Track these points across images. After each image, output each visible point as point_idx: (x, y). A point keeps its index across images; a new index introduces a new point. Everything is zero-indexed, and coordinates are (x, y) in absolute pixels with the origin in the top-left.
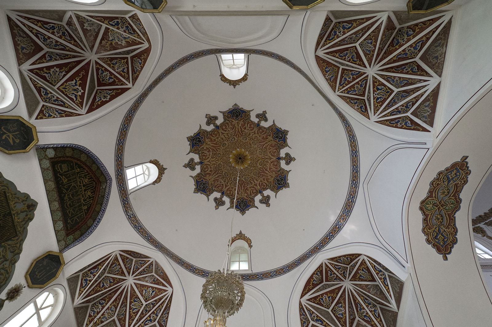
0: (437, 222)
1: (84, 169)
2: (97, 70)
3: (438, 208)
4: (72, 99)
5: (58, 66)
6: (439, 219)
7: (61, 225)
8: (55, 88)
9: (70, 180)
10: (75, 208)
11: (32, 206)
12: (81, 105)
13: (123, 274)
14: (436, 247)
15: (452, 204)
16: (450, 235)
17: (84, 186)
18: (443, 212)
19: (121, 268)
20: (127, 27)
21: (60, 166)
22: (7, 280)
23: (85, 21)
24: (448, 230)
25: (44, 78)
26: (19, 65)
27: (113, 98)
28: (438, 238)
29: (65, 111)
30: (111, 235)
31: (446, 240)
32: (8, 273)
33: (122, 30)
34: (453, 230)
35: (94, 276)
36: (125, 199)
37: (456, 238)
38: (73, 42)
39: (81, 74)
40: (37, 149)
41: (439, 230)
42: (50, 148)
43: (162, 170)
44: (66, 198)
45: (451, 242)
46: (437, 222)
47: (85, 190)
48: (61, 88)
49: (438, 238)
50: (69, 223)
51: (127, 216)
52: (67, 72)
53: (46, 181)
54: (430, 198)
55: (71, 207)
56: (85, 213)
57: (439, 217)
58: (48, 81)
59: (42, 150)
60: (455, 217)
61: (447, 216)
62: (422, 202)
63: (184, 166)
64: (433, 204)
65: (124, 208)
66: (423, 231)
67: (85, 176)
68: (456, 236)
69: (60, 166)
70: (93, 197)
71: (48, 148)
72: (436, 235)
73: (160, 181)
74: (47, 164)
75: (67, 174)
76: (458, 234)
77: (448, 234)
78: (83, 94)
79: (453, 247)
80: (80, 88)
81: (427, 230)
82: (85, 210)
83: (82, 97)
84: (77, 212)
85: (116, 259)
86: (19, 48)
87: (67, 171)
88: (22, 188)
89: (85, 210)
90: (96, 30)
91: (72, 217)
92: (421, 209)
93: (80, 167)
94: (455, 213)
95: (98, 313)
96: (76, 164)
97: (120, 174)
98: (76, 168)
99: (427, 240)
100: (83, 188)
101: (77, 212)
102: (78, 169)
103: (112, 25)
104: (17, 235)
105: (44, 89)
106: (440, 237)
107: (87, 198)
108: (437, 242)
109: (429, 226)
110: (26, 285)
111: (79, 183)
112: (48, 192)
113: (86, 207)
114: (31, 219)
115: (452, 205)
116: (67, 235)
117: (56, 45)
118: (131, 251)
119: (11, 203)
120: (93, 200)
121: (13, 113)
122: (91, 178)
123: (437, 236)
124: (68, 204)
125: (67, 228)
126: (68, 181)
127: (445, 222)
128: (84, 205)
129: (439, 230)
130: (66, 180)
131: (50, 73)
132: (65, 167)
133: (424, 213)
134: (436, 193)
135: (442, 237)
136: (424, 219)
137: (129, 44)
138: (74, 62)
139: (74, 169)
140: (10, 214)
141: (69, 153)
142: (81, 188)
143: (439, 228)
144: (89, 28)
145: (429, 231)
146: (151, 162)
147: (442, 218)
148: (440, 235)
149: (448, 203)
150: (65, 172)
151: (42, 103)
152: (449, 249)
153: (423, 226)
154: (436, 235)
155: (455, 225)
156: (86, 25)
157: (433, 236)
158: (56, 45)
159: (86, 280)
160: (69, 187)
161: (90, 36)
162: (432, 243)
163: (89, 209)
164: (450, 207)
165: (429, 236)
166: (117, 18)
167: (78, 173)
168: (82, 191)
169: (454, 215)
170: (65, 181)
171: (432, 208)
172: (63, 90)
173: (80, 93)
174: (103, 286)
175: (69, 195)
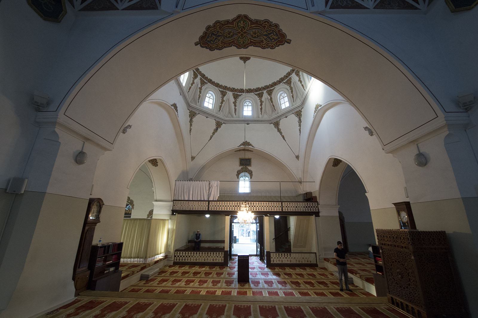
0: (226, 33)
3: (239, 32)
6: (229, 34)
14: (204, 35)
16: (216, 45)
18: (235, 37)
24: (220, 43)
28: (213, 36)
31: (212, 42)
34: (221, 46)
41: (219, 36)
46: (226, 33)
49: (213, 36)
54: (250, 23)
57: (231, 34)
60: (231, 46)
61: (233, 40)
62: (246, 17)
64: (243, 27)
68: (216, 50)
72: (215, 33)
76: (218, 51)
77: (217, 43)
79: (207, 48)
81: (218, 26)
92: (239, 16)
94: (235, 46)
99: (210, 27)
106: (214, 37)
108: (209, 35)
109: (222, 27)
115: (242, 42)
123: (214, 35)
129: (219, 36)
133: (234, 20)
134: (255, 27)
135: (214, 39)
136: (228, 21)
143: (221, 35)
145: (218, 27)
147: (231, 36)
149: (244, 39)
152: (205, 46)
153: (221, 21)
154: (215, 33)
155: (225, 47)
157: (213, 31)
162: (207, 32)
164: (240, 41)
165: (213, 28)
169: (233, 45)
171: (240, 27)
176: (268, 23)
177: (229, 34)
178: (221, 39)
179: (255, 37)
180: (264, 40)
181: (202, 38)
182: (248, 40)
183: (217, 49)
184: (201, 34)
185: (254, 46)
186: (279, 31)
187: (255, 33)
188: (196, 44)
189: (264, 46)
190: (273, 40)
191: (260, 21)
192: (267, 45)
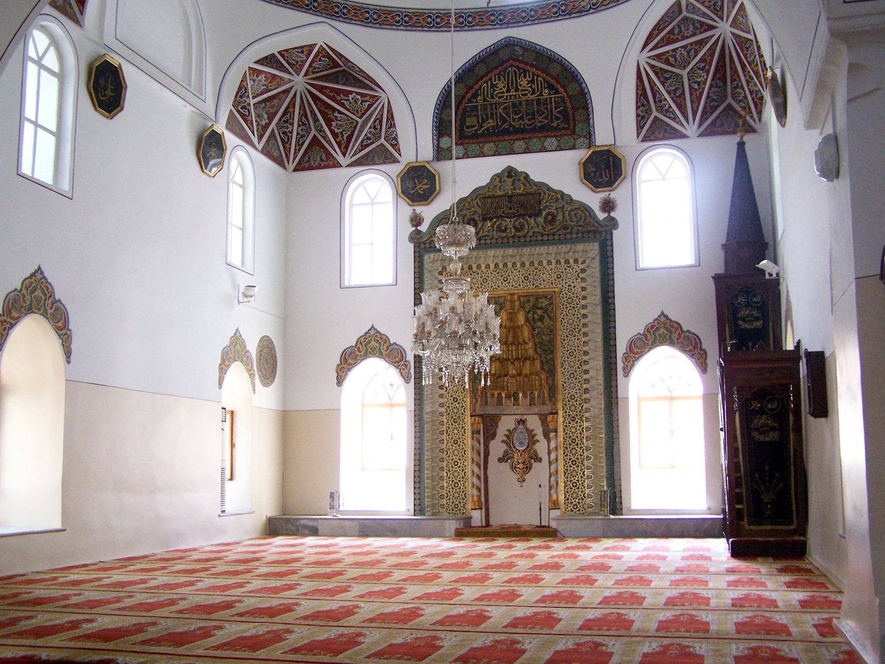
1: (480, 88)
2: (313, 73)
4: (370, 107)
5: (329, 126)
7: (551, 142)
8: (360, 121)
9: (492, 114)
10: (538, 111)
11: (510, 172)
12: (376, 98)
13: (701, 43)
17: (508, 91)
19: (685, 47)
20: (241, 97)
21: (467, 127)
22: (586, 209)
23: (260, 127)
25: (349, 138)
26: (341, 166)
27: (348, 61)
29: (388, 119)
32: (579, 208)
33: (247, 100)
35: (665, 99)
36: (555, 10)
38: (291, 110)
39: (331, 94)
40: (438, 159)
42: (438, 144)
44: (516, 124)
47: (517, 90)
48: (359, 115)
50: (558, 125)
51: (591, 11)
52: (334, 110)
53: (482, 155)
55: (534, 118)
56: (554, 94)
58: (353, 132)
59: (441, 154)
65: (573, 15)
67: (493, 86)
69: (467, 127)
70: (533, 74)
71: (438, 144)
75: (482, 117)
78: (358, 93)
80: (351, 97)
82: (550, 94)
83: (362, 95)
84: (546, 109)
85: (658, 57)
86: (322, 164)
87: (477, 115)
88: (484, 181)
89: (550, 94)
90: (263, 105)
91: (552, 119)
93: (475, 95)
95: (746, 97)
96: (470, 101)
97: (501, 17)
98: (477, 102)
100: (513, 92)
101: (546, 109)
102: (479, 98)
103: (249, 112)
104: (540, 194)
105: (363, 141)
107: (531, 87)
110: (607, 193)
111: (501, 100)
112: (497, 153)
113: (547, 91)
114: (527, 176)
116: (573, 132)
117: (304, 124)
118: (654, 29)
119: (499, 193)
120: (538, 76)
122: (499, 74)
124: (528, 122)
125: (564, 128)
126: (492, 118)
128: (541, 94)
130: (490, 121)
131: (341, 133)
137: (259, 72)
138: (316, 105)
139: (477, 106)
140: (510, 197)
142: (511, 96)
144: (266, 116)
150: (478, 122)
151: (382, 141)
156: (263, 123)
158: (304, 124)
159: (667, 111)
160: (502, 117)
161: (273, 106)
163: (550, 87)
166: (238, 111)
167: (485, 100)
168: (515, 96)
170: (491, 123)
172: (360, 113)
173: (359, 97)
174: (699, 83)
175: (514, 120)
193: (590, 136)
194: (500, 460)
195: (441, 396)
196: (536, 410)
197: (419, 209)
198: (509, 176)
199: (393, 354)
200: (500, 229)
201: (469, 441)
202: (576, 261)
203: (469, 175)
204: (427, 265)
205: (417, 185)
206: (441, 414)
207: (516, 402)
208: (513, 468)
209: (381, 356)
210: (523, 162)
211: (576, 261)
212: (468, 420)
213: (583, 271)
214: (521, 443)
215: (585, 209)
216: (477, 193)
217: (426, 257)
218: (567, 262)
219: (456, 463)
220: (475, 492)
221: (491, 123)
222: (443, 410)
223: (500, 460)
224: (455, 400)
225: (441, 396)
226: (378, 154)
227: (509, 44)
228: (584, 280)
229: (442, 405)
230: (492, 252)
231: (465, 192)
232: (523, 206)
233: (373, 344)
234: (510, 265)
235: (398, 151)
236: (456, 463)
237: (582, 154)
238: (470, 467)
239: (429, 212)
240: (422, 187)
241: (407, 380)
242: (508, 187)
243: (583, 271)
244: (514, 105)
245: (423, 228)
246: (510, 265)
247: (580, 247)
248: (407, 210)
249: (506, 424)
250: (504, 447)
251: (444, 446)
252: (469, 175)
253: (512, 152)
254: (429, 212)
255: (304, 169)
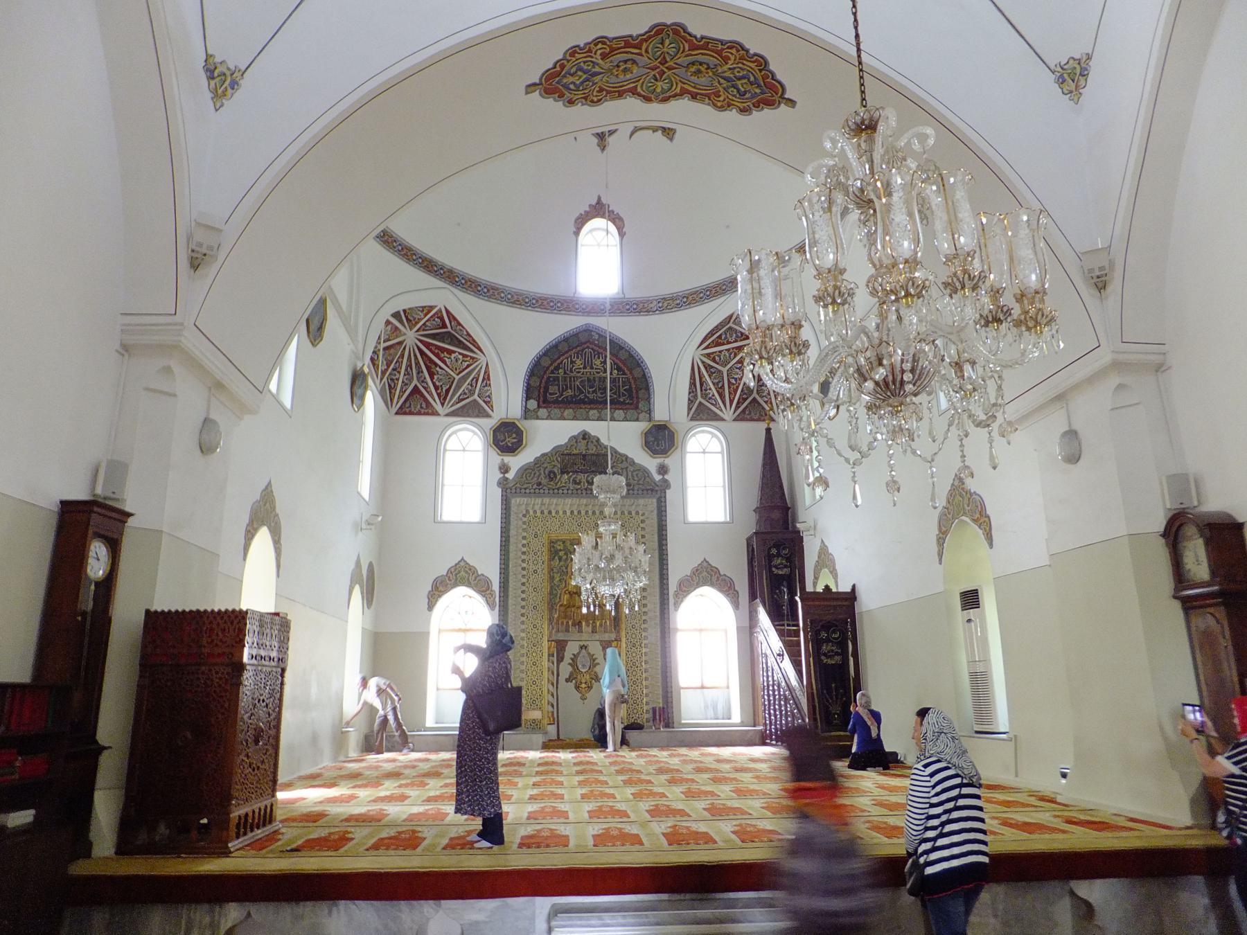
11: (585, 436)
15: (662, 43)
18: (683, 60)
30: (669, 353)
31: (752, 79)
34: (734, 51)
37: (756, 55)
43: (599, 209)
44: (591, 396)
45: (760, 71)
53: (563, 418)
59: (527, 414)
60: (702, 38)
63: (603, 149)
66: (721, 108)
67: (572, 362)
73: (621, 219)
74: (543, 412)
76: (747, 46)
88: (563, 440)
93: (557, 368)
94: (690, 35)
96: (552, 372)
108: (753, 97)
112: (575, 418)
114: (598, 440)
115: (667, 42)
116: (637, 408)
121: (487, 431)
123: (738, 90)
127: (712, 61)
132: (552, 389)
140: (584, 456)
141: (535, 382)
146: (577, 233)
148: (739, 83)
155: (722, 42)
170: (570, 392)
176: (592, 101)
177: (699, 71)
178: (725, 68)
179: (625, 62)
180: (600, 61)
181: (770, 103)
182: (647, 51)
183: (747, 51)
184: (767, 112)
185: (631, 36)
186: (561, 96)
187: (625, 70)
188: (791, 103)
189: (600, 46)
190: (574, 70)
191: (612, 99)
192: (590, 51)
193: (649, 412)
194: (567, 680)
195: (523, 623)
196: (597, 636)
197: (508, 459)
198: (584, 438)
199: (481, 586)
200: (575, 482)
201: (546, 663)
202: (637, 513)
203: (550, 434)
204: (514, 509)
205: (506, 438)
206: (523, 639)
207: (580, 631)
208: (577, 688)
209: (469, 585)
210: (595, 428)
211: (637, 513)
212: (546, 644)
213: (643, 521)
214: (584, 666)
215: (644, 472)
216: (557, 451)
217: (513, 501)
218: (630, 513)
219: (534, 683)
220: (550, 709)
221: (570, 392)
222: (523, 635)
223: (567, 680)
224: (535, 626)
225: (523, 623)
226: (472, 410)
227: (588, 330)
228: (643, 529)
229: (523, 631)
230: (569, 501)
231: (547, 449)
232: (594, 463)
233: (462, 575)
234: (583, 513)
235: (492, 408)
236: (534, 683)
237: (643, 426)
238: (546, 686)
239: (517, 462)
240: (510, 441)
241: (491, 606)
242: (582, 447)
243: (643, 521)
244: (589, 380)
245: (510, 475)
246: (583, 513)
247: (641, 501)
248: (496, 458)
249: (572, 649)
250: (570, 669)
251: (523, 667)
252: (550, 434)
253: (587, 419)
254: (517, 462)
255: (405, 413)
